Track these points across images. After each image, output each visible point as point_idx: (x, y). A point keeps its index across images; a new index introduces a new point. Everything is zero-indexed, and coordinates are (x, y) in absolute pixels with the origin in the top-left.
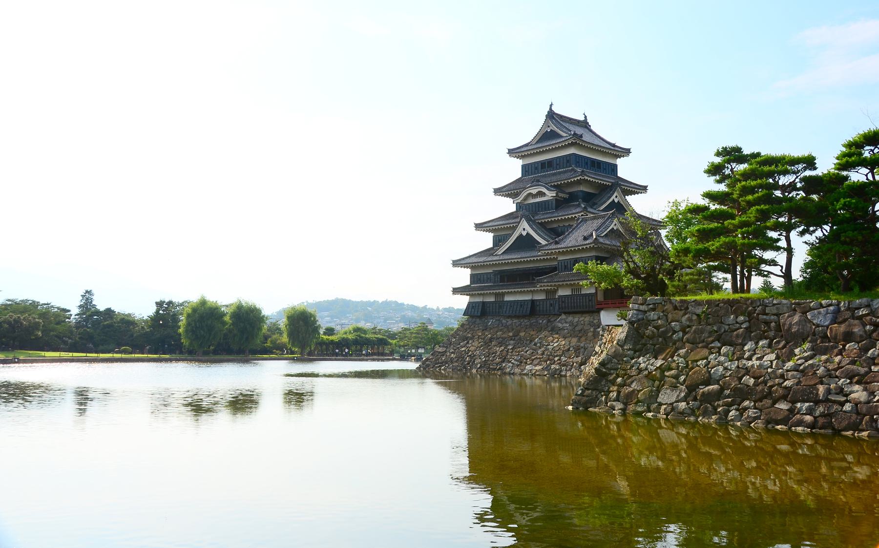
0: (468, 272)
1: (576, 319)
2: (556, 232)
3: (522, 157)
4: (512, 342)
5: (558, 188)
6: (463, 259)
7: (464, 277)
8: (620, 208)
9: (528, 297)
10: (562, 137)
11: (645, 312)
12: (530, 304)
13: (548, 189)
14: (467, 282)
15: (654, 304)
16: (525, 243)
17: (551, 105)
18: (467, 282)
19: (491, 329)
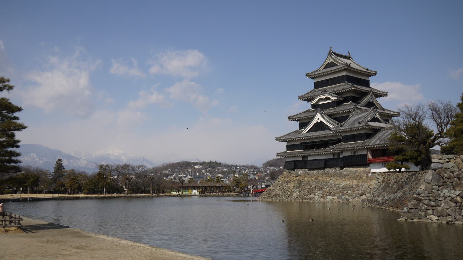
0: (285, 144)
1: (355, 169)
3: (313, 78)
5: (338, 94)
7: (283, 147)
9: (323, 157)
11: (443, 163)
13: (332, 96)
15: (449, 159)
16: (320, 126)
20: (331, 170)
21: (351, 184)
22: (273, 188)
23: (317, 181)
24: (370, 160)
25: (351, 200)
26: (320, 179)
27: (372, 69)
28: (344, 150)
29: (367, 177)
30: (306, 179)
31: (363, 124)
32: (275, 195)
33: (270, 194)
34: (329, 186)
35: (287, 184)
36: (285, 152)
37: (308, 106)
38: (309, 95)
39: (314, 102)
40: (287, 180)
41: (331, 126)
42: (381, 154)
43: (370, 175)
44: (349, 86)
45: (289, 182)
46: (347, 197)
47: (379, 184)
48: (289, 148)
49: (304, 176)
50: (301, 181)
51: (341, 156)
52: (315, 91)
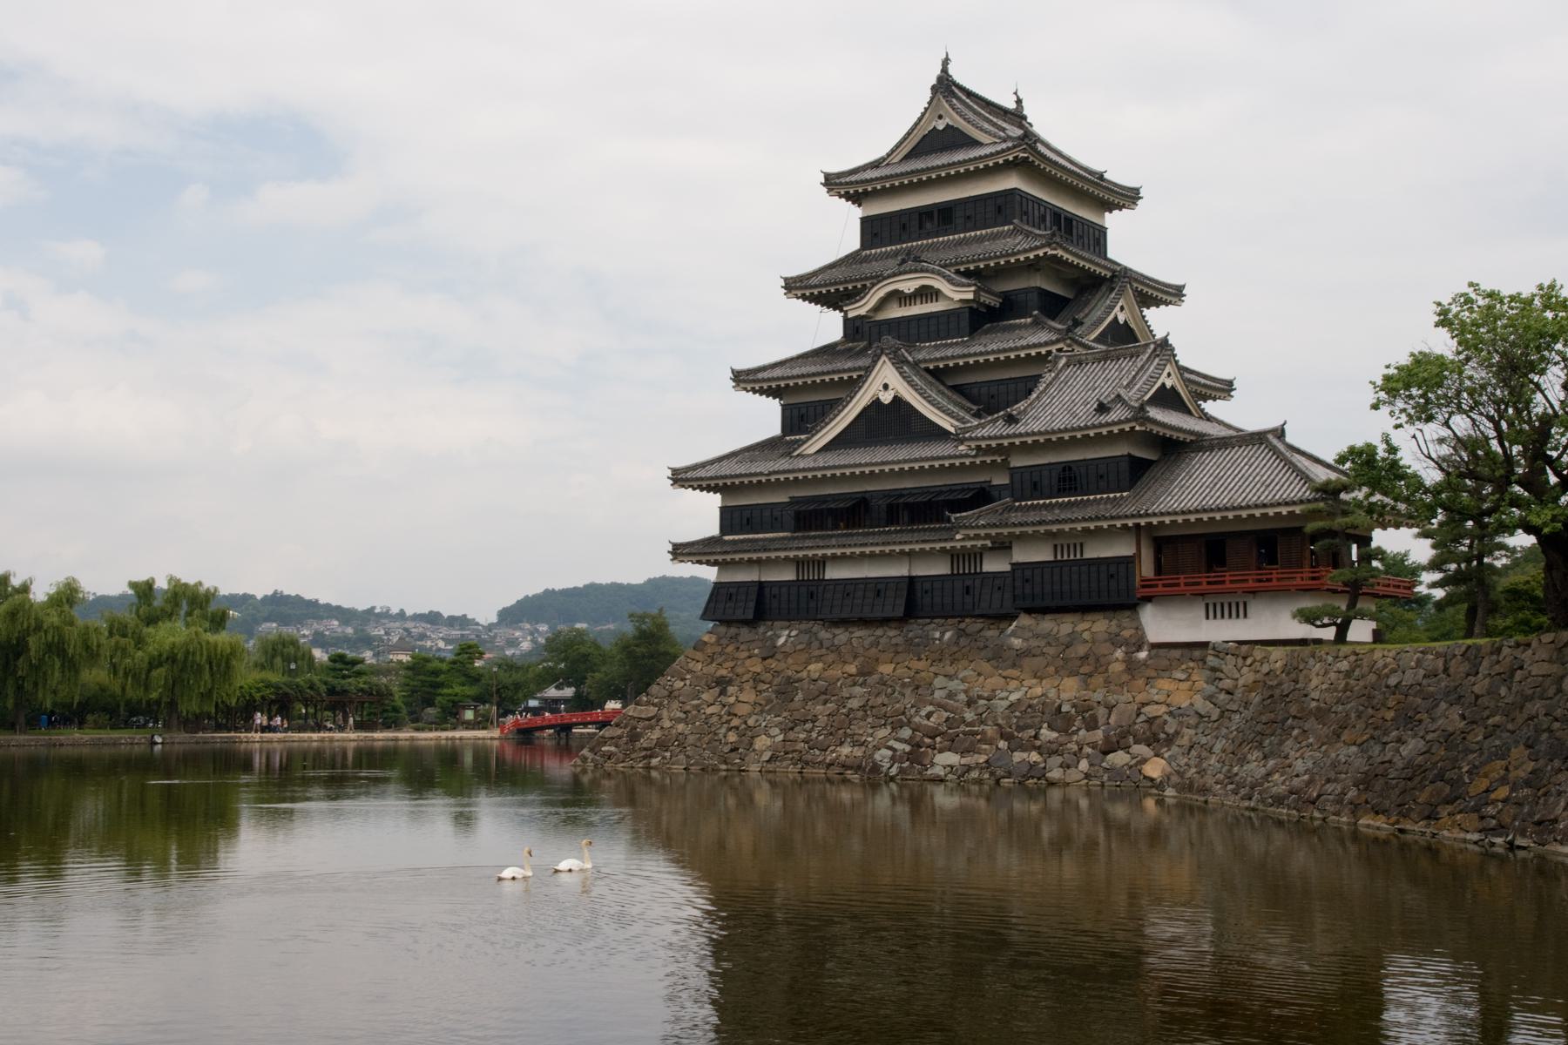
0: (714, 501)
1: (1065, 626)
2: (991, 395)
3: (856, 198)
4: (858, 690)
6: (703, 465)
7: (702, 514)
8: (1123, 337)
9: (899, 570)
10: (976, 144)
12: (904, 586)
13: (950, 281)
14: (712, 528)
16: (890, 422)
17: (946, 62)
18: (712, 528)
19: (787, 655)
21: (1052, 694)
22: (653, 710)
23: (872, 679)
24: (1147, 583)
25: (1055, 774)
26: (886, 669)
27: (1118, 175)
29: (1131, 666)
32: (662, 744)
33: (634, 737)
34: (940, 706)
35: (723, 692)
36: (709, 542)
37: (827, 326)
38: (837, 274)
39: (861, 309)
40: (723, 672)
41: (946, 423)
42: (1224, 557)
43: (1143, 655)
45: (730, 682)
46: (1034, 757)
48: (730, 519)
49: (803, 657)
50: (789, 681)
51: (994, 565)
52: (867, 260)
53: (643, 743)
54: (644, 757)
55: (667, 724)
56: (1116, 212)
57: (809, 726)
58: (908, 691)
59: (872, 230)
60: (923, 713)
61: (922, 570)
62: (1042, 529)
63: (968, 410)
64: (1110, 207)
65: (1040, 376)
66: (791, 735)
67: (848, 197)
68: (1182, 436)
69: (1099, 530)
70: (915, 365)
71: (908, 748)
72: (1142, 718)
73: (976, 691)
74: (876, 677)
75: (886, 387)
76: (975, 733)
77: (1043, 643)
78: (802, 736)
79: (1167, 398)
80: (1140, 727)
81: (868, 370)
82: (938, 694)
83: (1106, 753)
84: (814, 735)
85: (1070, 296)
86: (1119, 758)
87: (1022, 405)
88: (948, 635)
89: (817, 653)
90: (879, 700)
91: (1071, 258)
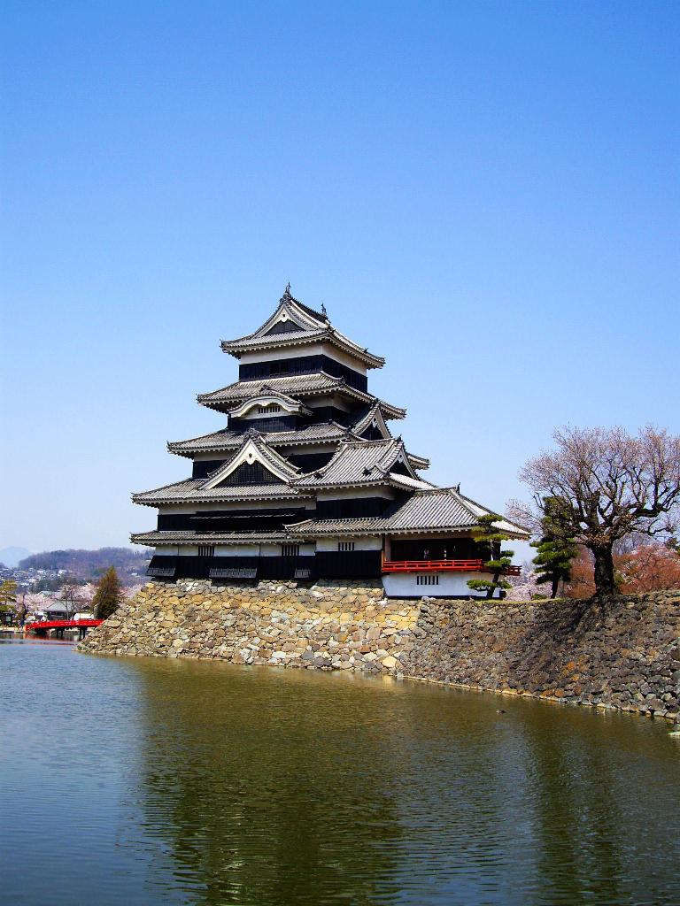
0: (156, 511)
3: (238, 355)
7: (148, 519)
19: (192, 596)
20: (277, 588)
22: (118, 623)
25: (337, 664)
26: (245, 606)
28: (322, 538)
30: (207, 603)
31: (375, 475)
32: (122, 642)
33: (107, 637)
37: (221, 421)
38: (226, 394)
39: (239, 413)
40: (157, 604)
44: (316, 383)
45: (160, 610)
46: (326, 654)
47: (428, 625)
48: (164, 523)
49: (201, 597)
50: (193, 610)
51: (305, 552)
52: (241, 388)
53: (112, 640)
54: (113, 648)
55: (125, 630)
56: (372, 369)
57: (203, 635)
58: (257, 618)
59: (247, 373)
60: (267, 630)
61: (268, 553)
62: (333, 534)
63: (294, 470)
64: (369, 366)
65: (333, 454)
66: (194, 639)
67: (233, 354)
68: (407, 488)
69: (363, 536)
70: (267, 444)
71: (258, 649)
72: (383, 635)
73: (296, 619)
74: (239, 610)
75: (250, 456)
76: (294, 642)
77: (331, 595)
78: (200, 640)
79: (399, 468)
80: (382, 641)
81: (241, 446)
82: (273, 620)
83: (364, 653)
84: (206, 640)
85: (348, 412)
86: (371, 656)
87: (323, 469)
88: (279, 589)
89: (208, 595)
90: (242, 622)
91: (350, 393)
